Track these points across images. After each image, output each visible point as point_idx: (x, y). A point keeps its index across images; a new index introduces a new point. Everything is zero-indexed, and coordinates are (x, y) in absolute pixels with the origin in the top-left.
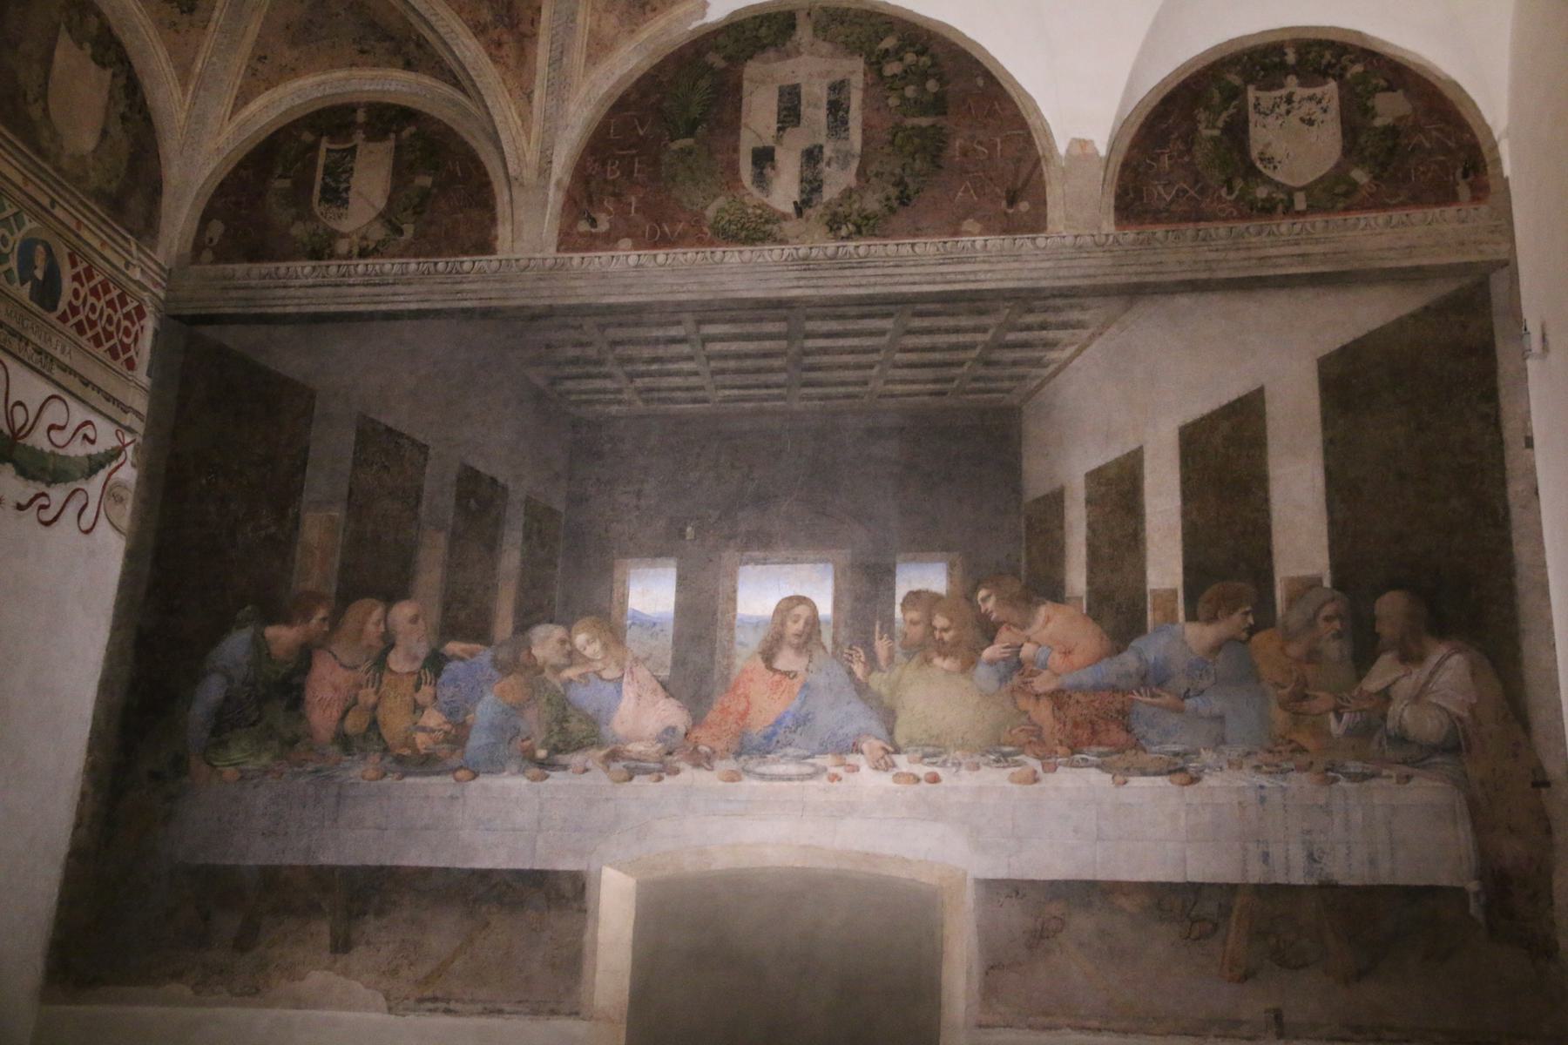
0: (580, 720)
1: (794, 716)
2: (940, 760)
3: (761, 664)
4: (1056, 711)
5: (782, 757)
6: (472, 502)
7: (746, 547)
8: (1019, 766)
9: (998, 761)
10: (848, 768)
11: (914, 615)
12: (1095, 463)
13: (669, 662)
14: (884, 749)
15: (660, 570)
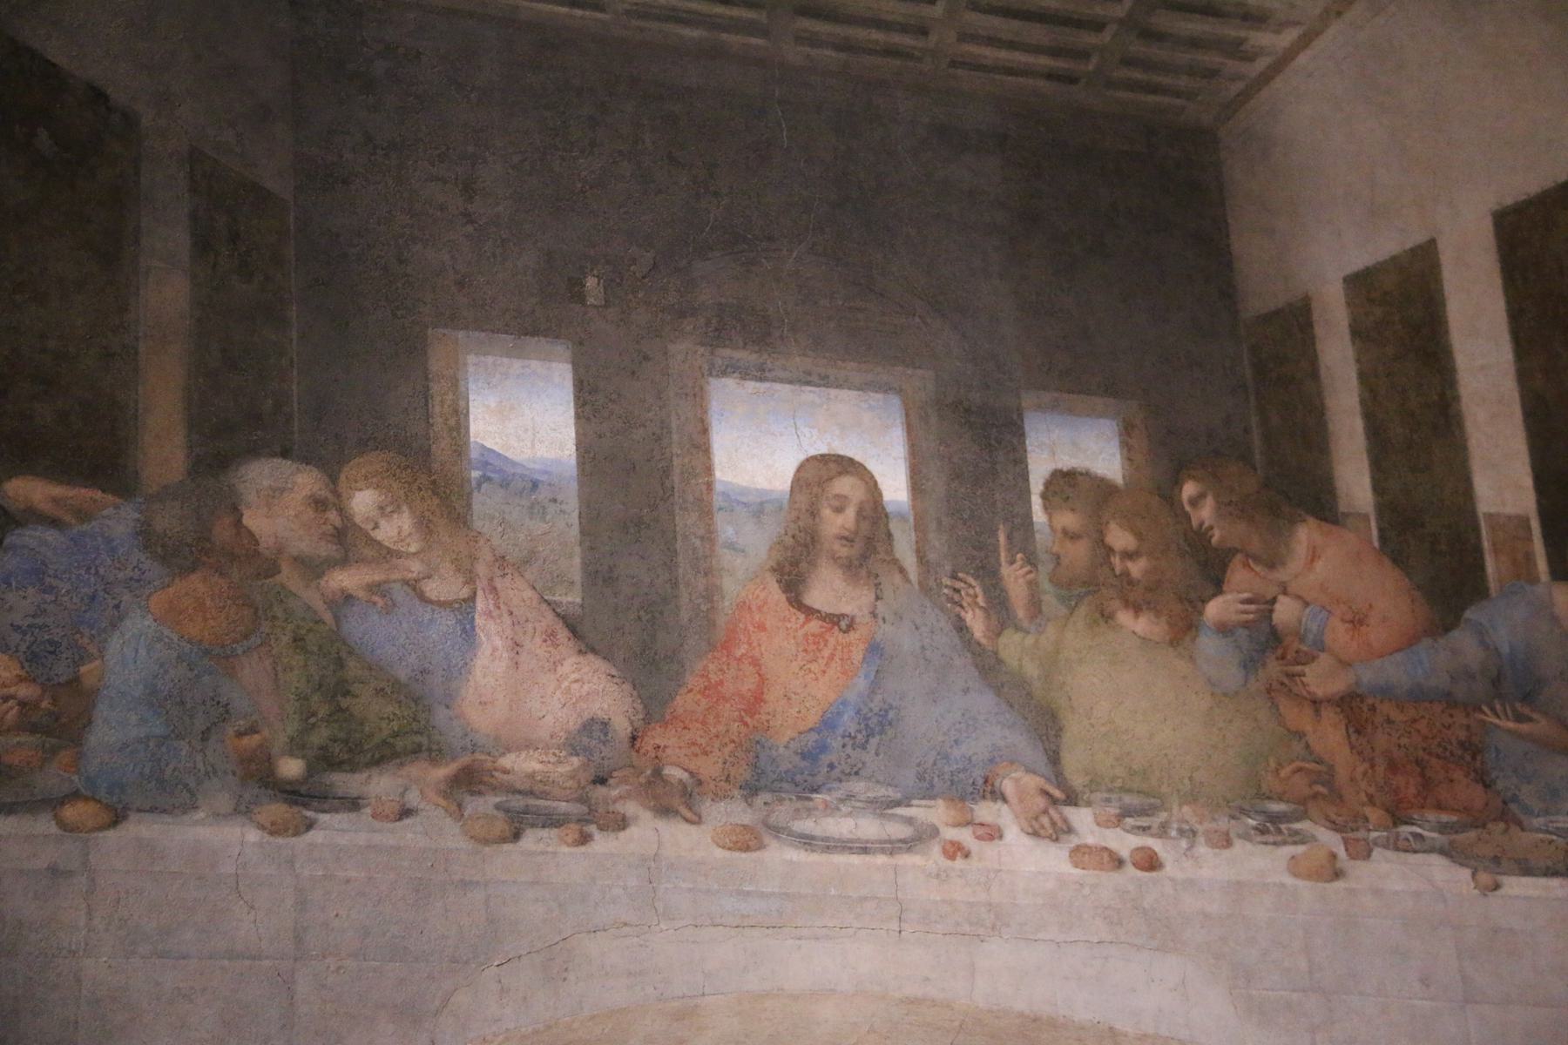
0: (380, 692)
1: (858, 712)
2: (1155, 821)
3: (775, 594)
4: (1354, 737)
5: (842, 801)
6: (43, 135)
7: (717, 335)
8: (1303, 842)
9: (1262, 831)
10: (981, 831)
11: (1068, 520)
12: (1360, 258)
13: (576, 573)
14: (1046, 793)
15: (535, 364)
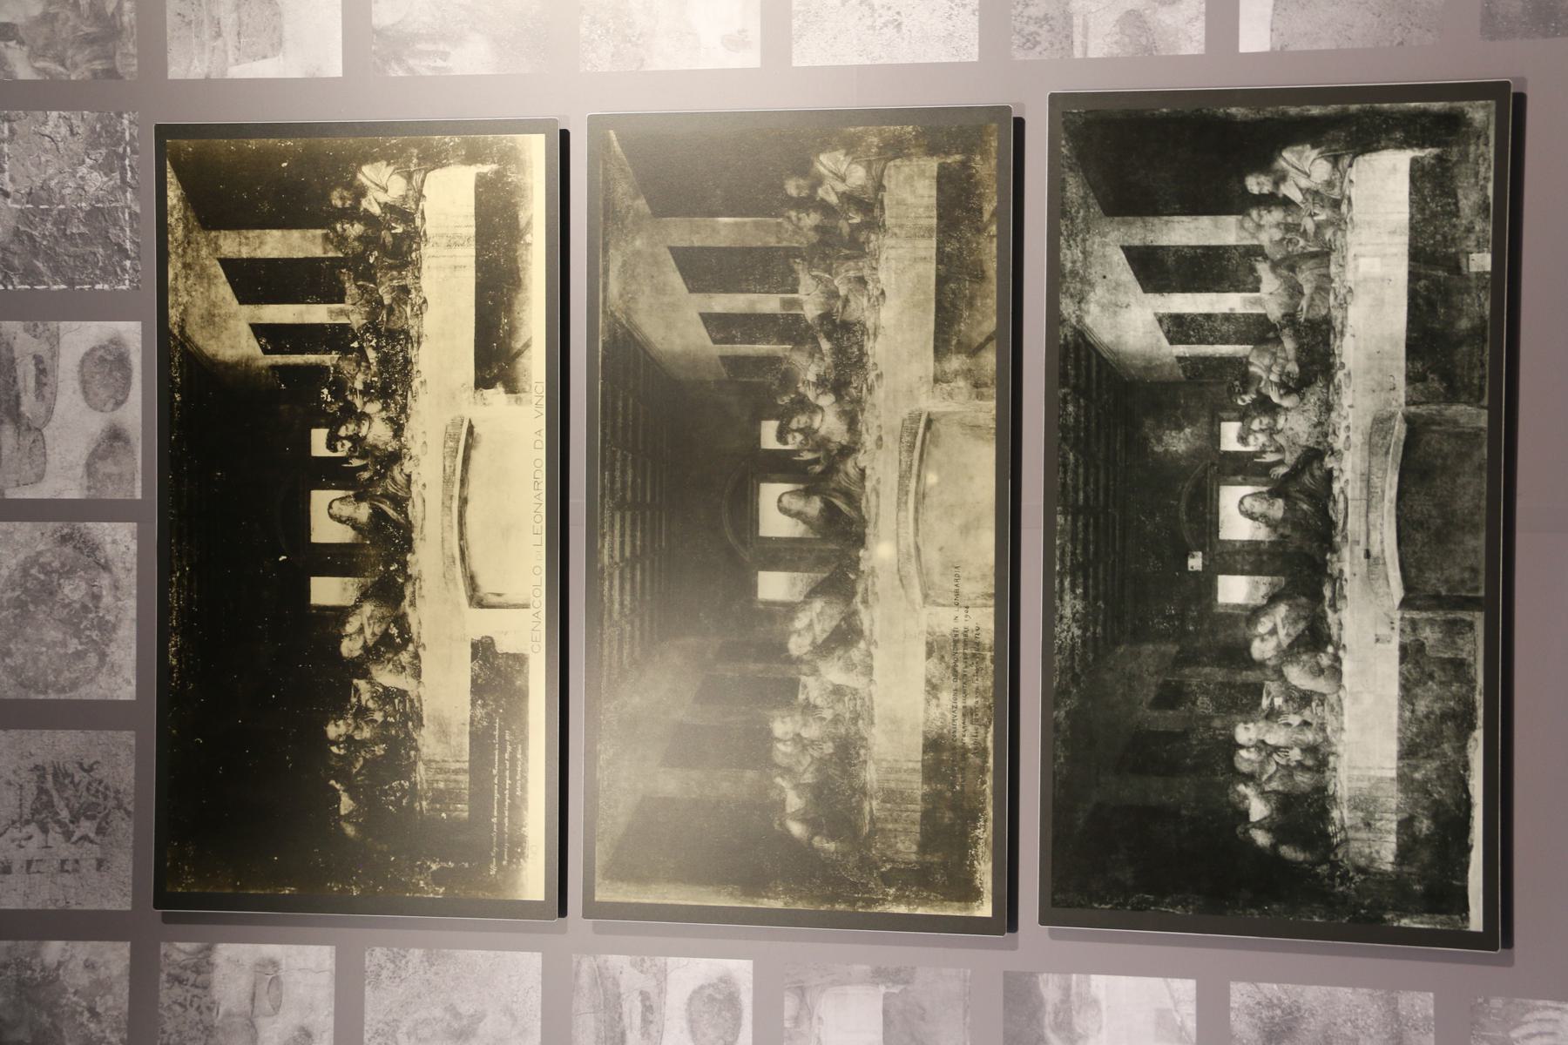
10: (265, 1004)
